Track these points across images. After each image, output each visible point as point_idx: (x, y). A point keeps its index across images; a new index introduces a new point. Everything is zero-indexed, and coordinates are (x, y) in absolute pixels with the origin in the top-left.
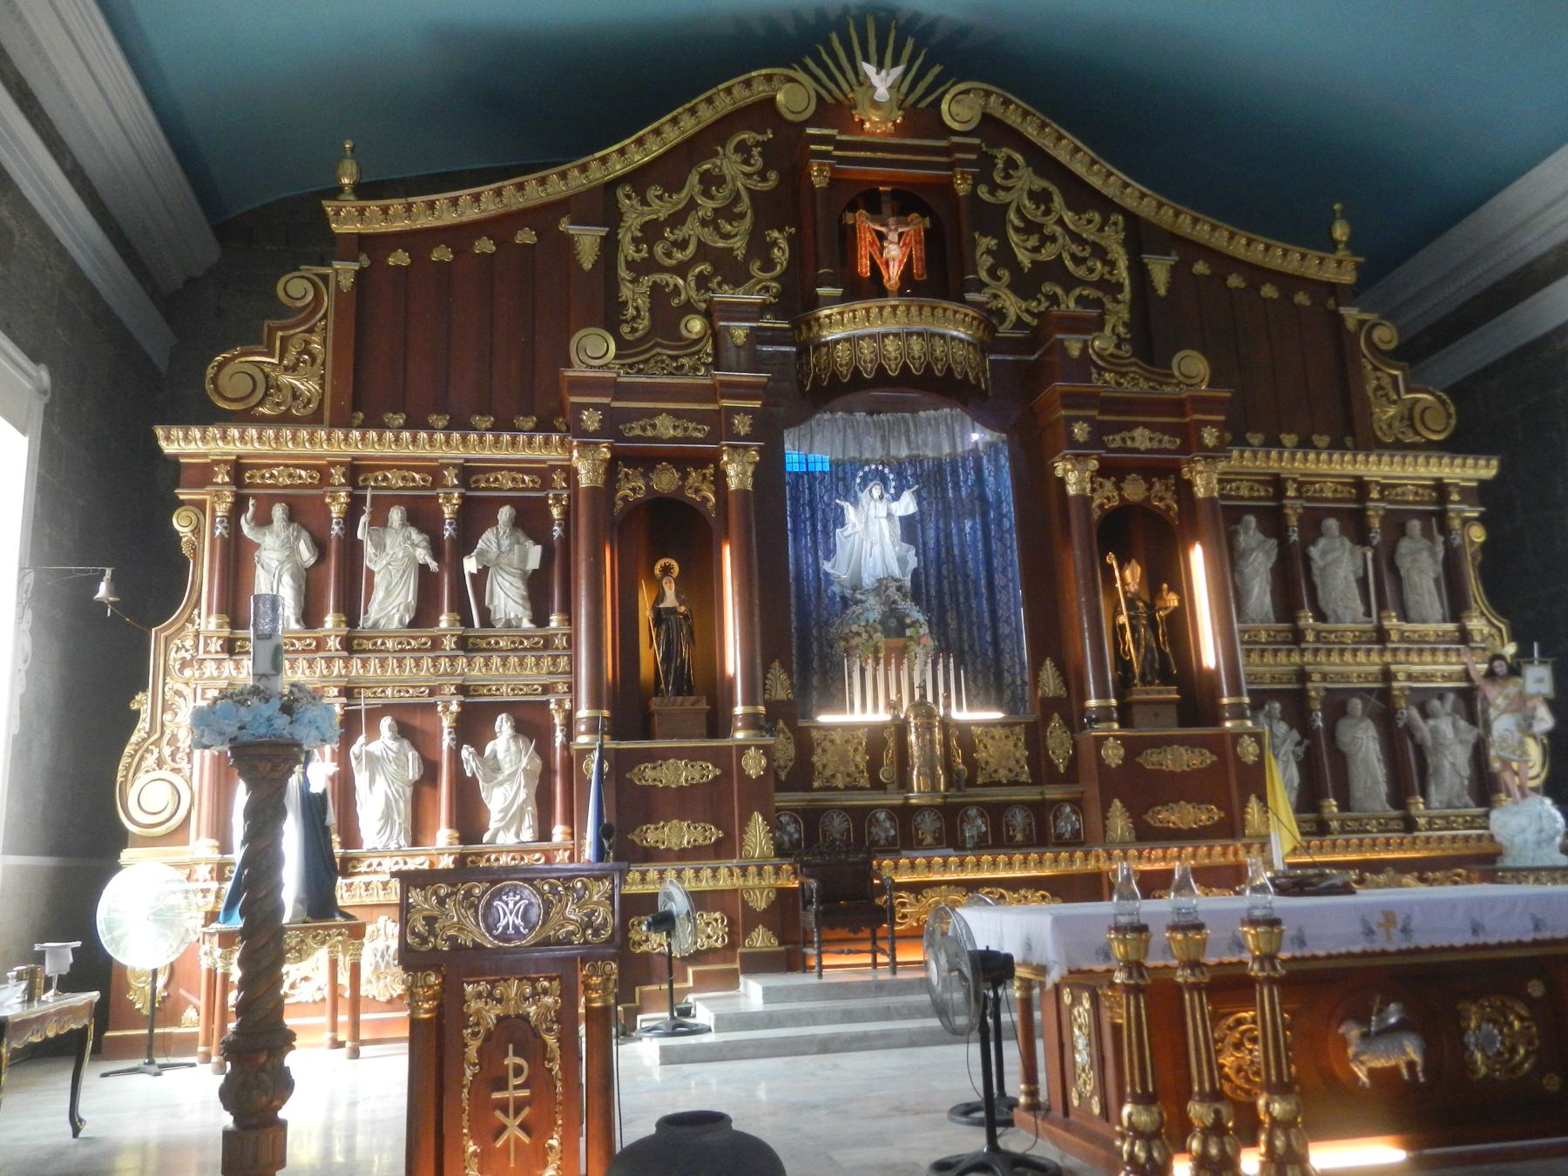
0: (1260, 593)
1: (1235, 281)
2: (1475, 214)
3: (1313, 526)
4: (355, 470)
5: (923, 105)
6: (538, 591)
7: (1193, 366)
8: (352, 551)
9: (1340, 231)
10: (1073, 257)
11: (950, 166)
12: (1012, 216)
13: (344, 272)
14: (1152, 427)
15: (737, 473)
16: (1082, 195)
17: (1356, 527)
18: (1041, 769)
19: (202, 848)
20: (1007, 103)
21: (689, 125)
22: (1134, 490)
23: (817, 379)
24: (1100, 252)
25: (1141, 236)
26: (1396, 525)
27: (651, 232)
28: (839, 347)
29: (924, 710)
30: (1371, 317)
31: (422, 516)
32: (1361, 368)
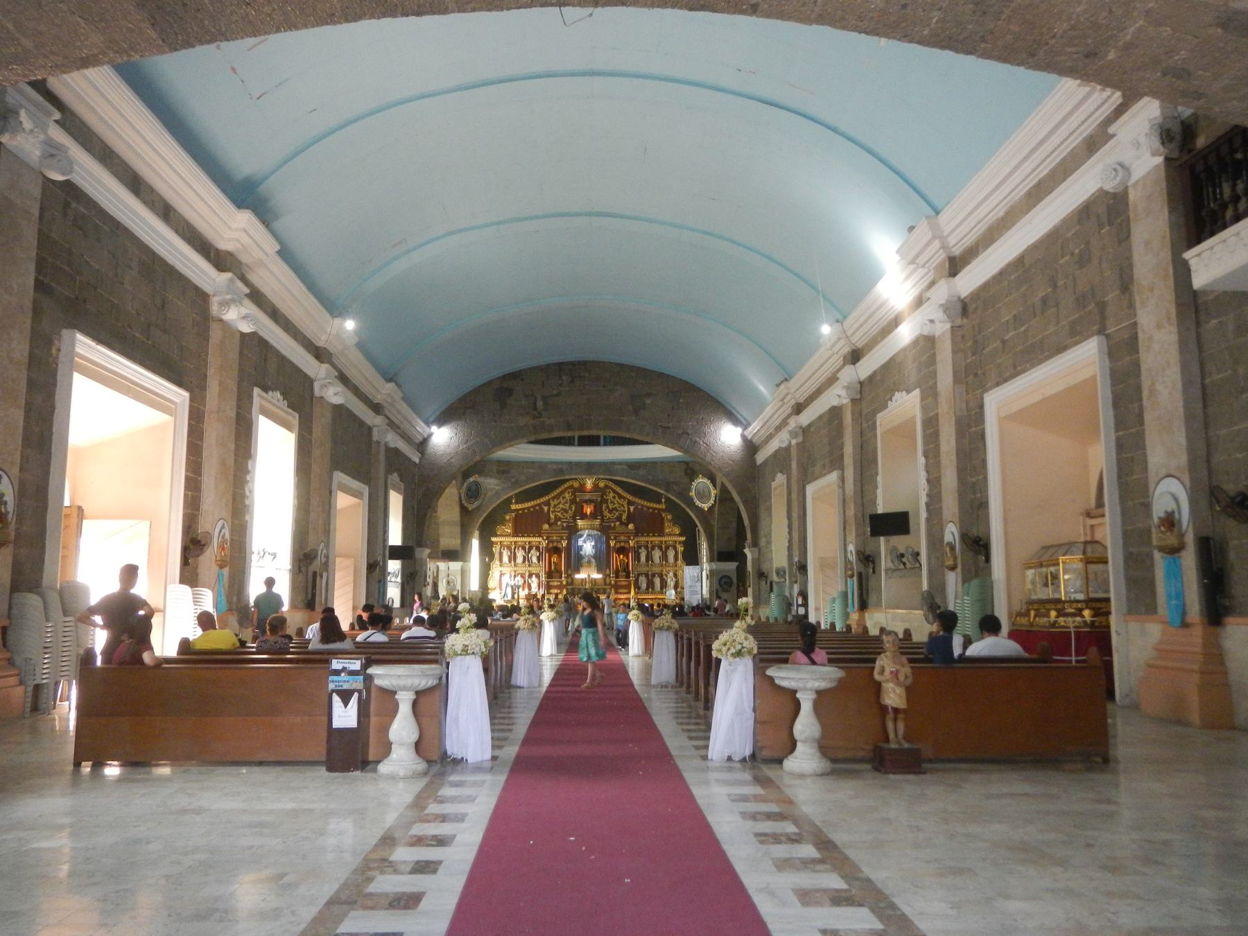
0: (643, 558)
3: (653, 548)
4: (515, 542)
6: (538, 559)
8: (515, 554)
9: (663, 500)
13: (513, 514)
15: (564, 544)
16: (620, 497)
17: (660, 548)
18: (605, 584)
19: (498, 590)
21: (560, 490)
22: (622, 544)
24: (623, 505)
26: (667, 548)
27: (555, 506)
29: (589, 576)
31: (524, 548)
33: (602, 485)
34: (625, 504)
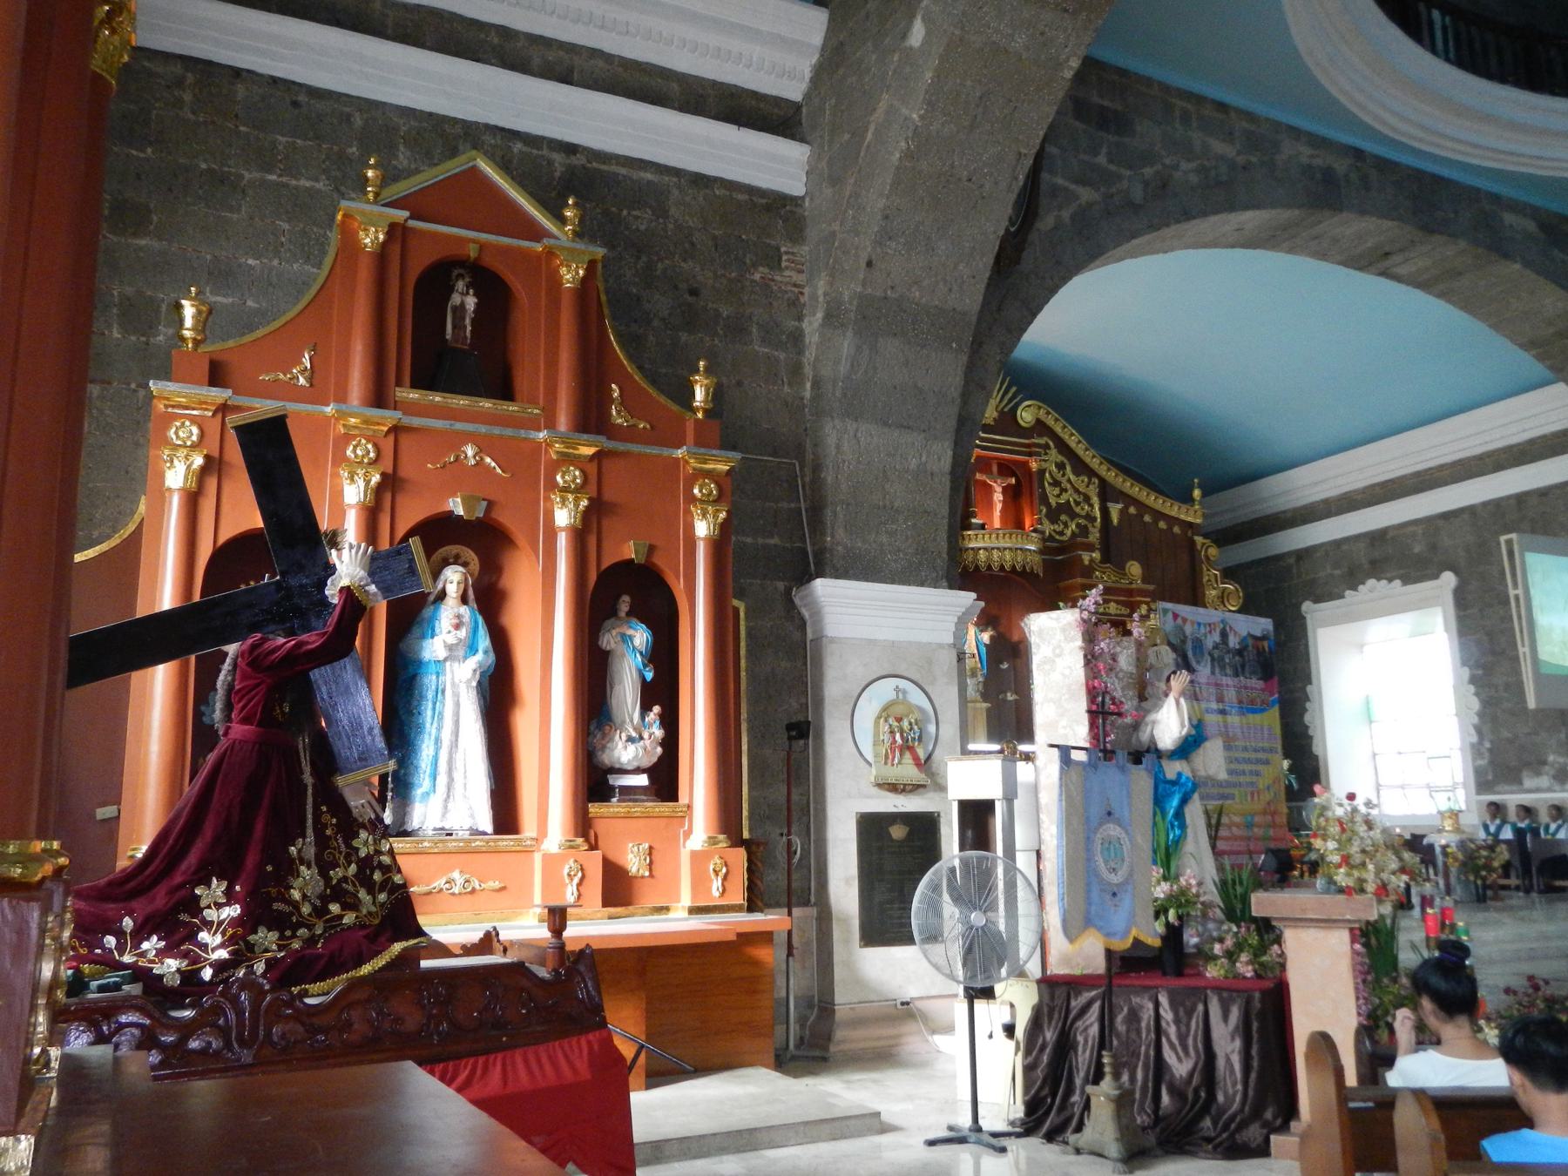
1: (1147, 518)
2: (1253, 484)
5: (1006, 410)
7: (1135, 569)
9: (1197, 493)
10: (1075, 501)
11: (1030, 454)
12: (1047, 475)
14: (1117, 602)
16: (1081, 467)
20: (1048, 413)
23: (965, 568)
24: (1087, 499)
25: (1107, 493)
28: (981, 552)
30: (1207, 541)
32: (1201, 569)
33: (1026, 416)
34: (1093, 492)
